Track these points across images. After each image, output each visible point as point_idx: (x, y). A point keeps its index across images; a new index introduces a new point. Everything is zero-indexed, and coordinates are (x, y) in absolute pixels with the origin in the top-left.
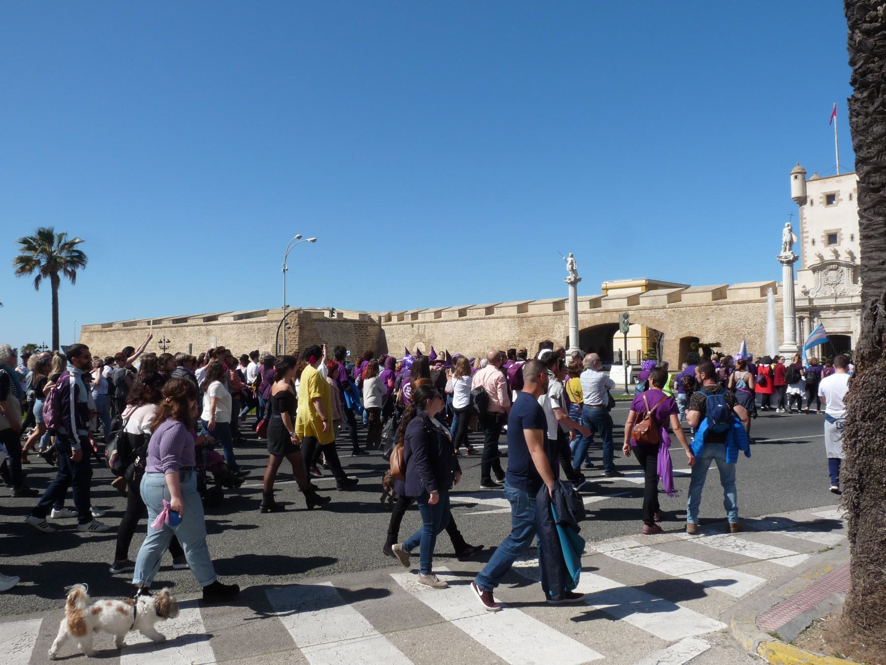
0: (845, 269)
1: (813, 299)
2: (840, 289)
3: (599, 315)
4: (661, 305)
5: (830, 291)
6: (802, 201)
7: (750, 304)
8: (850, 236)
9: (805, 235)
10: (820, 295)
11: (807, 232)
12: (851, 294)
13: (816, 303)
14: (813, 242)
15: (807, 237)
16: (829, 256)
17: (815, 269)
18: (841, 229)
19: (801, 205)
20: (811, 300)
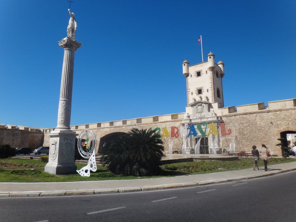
0: (204, 105)
1: (191, 120)
2: (203, 114)
3: (112, 128)
4: (134, 124)
5: (199, 115)
6: (187, 75)
7: (167, 123)
8: (207, 90)
9: (189, 90)
10: (194, 117)
11: (190, 89)
12: (207, 117)
13: (192, 121)
14: (192, 93)
15: (189, 91)
16: (198, 99)
17: (192, 106)
18: (203, 87)
19: (187, 77)
20: (190, 120)
